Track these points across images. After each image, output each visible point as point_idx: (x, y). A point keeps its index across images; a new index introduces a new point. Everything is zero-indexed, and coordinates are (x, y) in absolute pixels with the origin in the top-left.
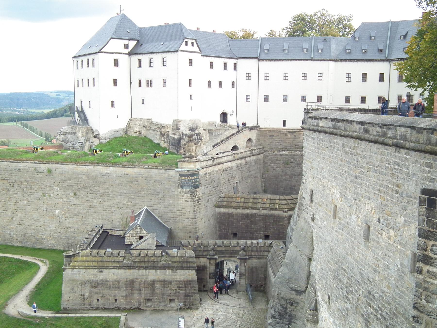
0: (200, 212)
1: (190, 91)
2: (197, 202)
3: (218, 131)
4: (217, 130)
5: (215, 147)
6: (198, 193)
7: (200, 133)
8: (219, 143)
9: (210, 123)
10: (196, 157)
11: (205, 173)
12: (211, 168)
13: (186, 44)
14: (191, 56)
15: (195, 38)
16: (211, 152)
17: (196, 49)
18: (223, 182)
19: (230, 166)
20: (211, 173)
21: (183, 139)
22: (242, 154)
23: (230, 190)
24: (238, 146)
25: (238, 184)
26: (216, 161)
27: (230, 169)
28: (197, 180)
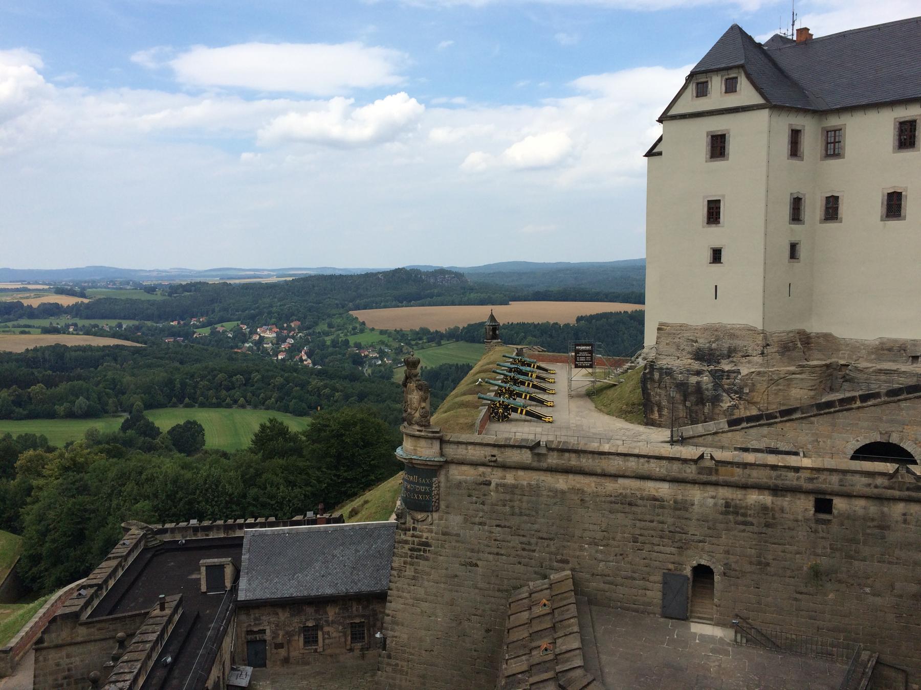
0: (414, 578)
1: (715, 236)
2: (407, 547)
3: (883, 377)
4: (880, 371)
5: (744, 425)
6: (418, 526)
7: (738, 372)
8: (770, 416)
9: (888, 346)
10: (418, 424)
11: (482, 479)
12: (521, 473)
13: (702, 91)
14: (717, 125)
15: (742, 62)
16: (717, 438)
17: (746, 94)
18: (587, 534)
19: (667, 497)
20: (514, 487)
21: (652, 380)
22: (791, 475)
23: (636, 575)
24: (908, 446)
25: (717, 578)
26: (553, 460)
27: (662, 507)
28: (423, 489)
